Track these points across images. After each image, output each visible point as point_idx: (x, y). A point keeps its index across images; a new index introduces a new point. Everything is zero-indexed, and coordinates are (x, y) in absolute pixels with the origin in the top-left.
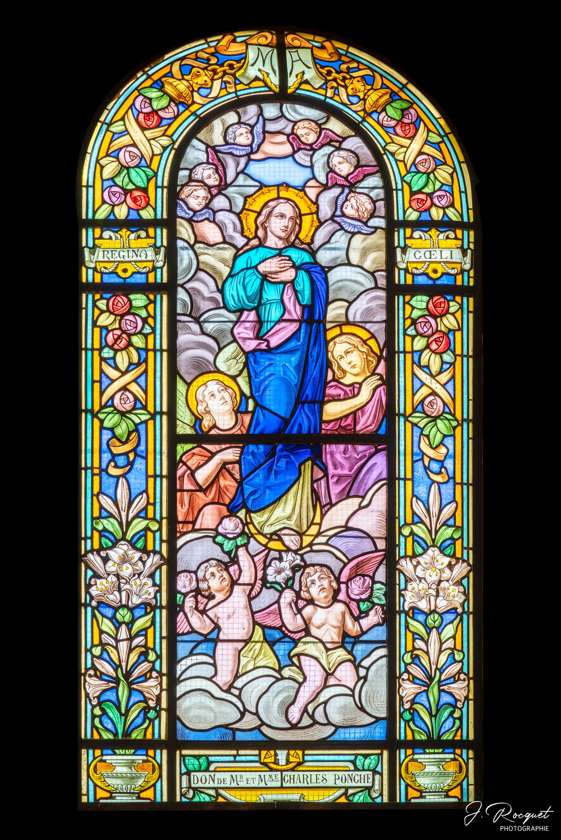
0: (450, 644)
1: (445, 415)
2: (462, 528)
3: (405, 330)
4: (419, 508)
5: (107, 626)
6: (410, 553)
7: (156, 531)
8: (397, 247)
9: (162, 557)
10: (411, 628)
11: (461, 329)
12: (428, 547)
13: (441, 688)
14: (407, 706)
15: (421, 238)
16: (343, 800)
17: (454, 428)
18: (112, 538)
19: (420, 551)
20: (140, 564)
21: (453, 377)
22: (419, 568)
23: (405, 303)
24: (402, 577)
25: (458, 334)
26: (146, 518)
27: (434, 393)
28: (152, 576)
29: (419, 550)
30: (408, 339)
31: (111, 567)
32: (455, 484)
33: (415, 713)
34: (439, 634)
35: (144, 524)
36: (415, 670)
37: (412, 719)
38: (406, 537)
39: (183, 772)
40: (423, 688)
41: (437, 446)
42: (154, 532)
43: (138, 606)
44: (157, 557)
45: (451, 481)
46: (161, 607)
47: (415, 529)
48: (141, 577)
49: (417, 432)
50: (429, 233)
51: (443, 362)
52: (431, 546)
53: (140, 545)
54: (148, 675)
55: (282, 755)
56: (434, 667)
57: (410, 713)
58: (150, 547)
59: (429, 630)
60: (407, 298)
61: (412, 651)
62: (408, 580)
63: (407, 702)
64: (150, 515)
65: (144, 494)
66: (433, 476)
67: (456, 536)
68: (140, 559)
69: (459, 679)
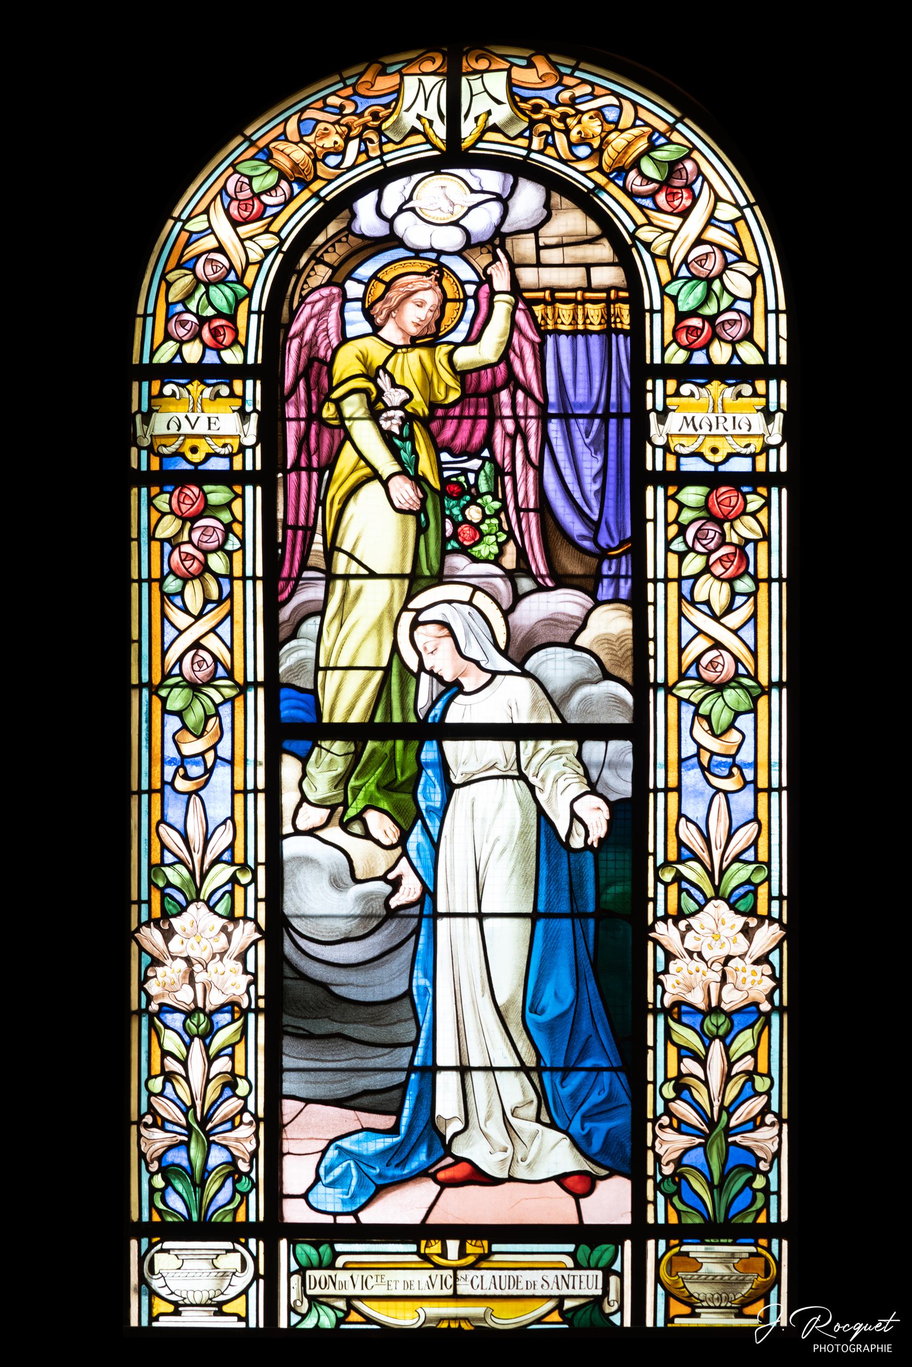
0: (747, 1063)
2: (768, 864)
3: (668, 543)
4: (689, 834)
6: (673, 909)
7: (249, 884)
8: (651, 411)
9: (258, 929)
10: (675, 1038)
11: (767, 537)
12: (708, 901)
15: (692, 395)
17: (755, 700)
19: (693, 907)
20: (223, 937)
22: (690, 935)
23: (667, 498)
25: (763, 547)
26: (232, 863)
27: (717, 645)
28: (242, 958)
29: (691, 906)
30: (673, 559)
32: (757, 791)
33: (683, 1182)
34: (727, 1048)
36: (682, 1109)
37: (678, 1193)
39: (292, 1270)
40: (698, 1141)
41: (724, 732)
44: (251, 925)
50: (708, 386)
52: (712, 898)
54: (237, 1120)
55: (453, 1246)
56: (716, 1104)
57: (674, 1182)
58: (239, 912)
59: (707, 1039)
60: (672, 490)
62: (670, 956)
63: (667, 1164)
64: (239, 859)
65: (229, 822)
66: (715, 781)
67: (757, 879)
68: (224, 929)
69: (763, 1124)
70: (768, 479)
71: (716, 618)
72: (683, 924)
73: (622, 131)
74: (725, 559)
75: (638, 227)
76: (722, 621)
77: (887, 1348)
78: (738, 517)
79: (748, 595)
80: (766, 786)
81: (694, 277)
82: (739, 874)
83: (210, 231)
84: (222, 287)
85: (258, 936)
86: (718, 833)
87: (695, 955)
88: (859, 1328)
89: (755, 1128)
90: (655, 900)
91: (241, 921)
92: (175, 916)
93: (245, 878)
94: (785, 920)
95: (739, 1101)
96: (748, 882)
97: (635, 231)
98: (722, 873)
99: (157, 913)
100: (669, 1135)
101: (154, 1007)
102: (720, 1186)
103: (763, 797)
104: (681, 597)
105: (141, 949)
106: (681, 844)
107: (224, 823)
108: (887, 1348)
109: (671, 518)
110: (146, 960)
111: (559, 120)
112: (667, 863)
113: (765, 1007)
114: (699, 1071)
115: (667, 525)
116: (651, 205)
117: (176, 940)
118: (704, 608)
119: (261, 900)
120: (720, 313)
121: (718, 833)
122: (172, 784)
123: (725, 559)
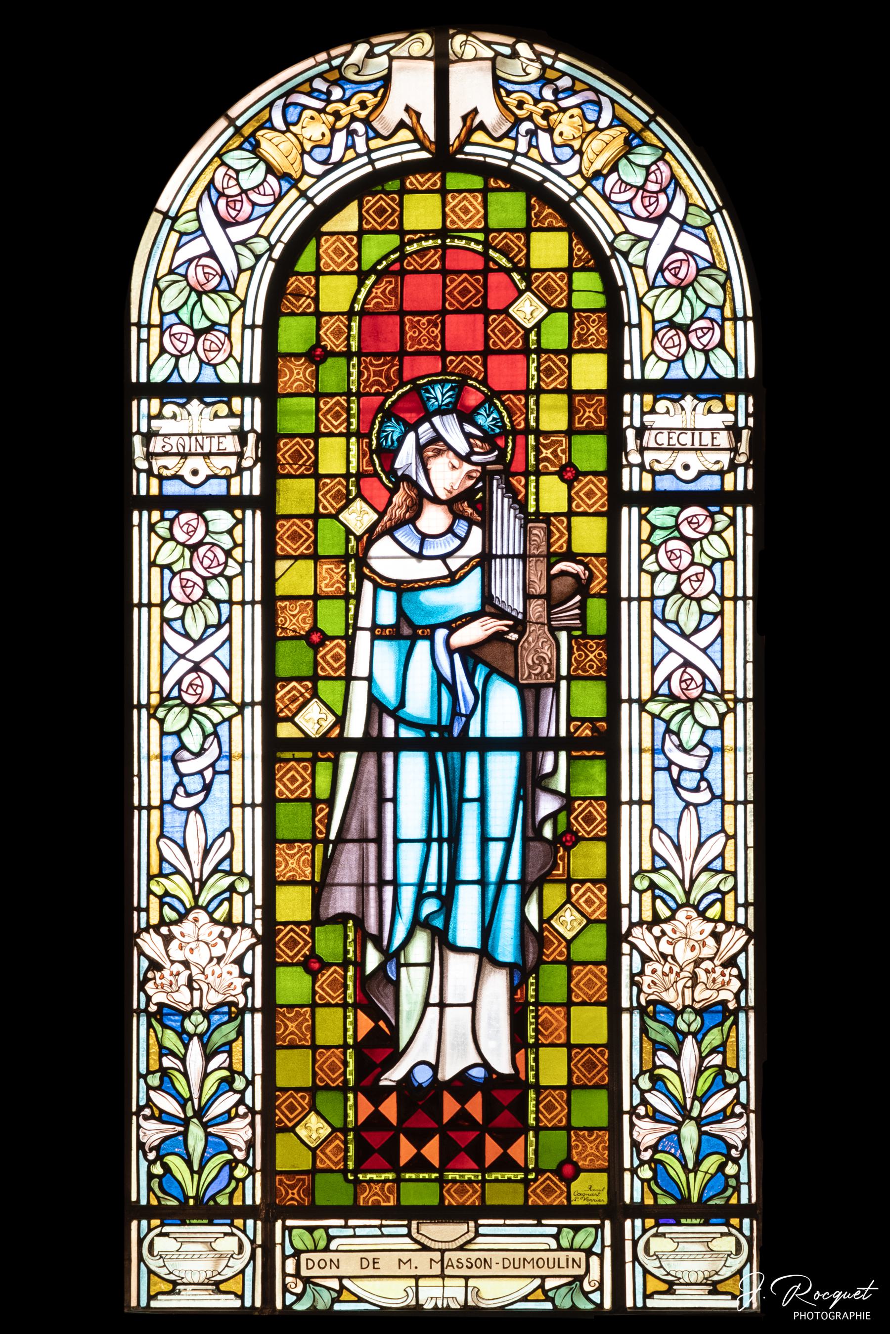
2: (734, 874)
3: (641, 562)
5: (171, 1040)
6: (648, 916)
7: (247, 893)
11: (733, 558)
13: (704, 1129)
14: (646, 1156)
17: (722, 717)
20: (221, 943)
21: (721, 634)
23: (642, 517)
25: (729, 565)
26: (230, 873)
27: (687, 664)
28: (239, 961)
29: (664, 912)
30: (646, 578)
31: (176, 953)
34: (699, 1043)
38: (641, 892)
44: (247, 932)
45: (717, 803)
46: (253, 1010)
48: (222, 964)
49: (660, 727)
50: (682, 402)
51: (702, 612)
53: (220, 915)
56: (689, 1095)
57: (651, 1168)
58: (237, 918)
60: (644, 510)
61: (651, 1071)
63: (646, 1150)
64: (237, 869)
65: (228, 834)
68: (221, 935)
70: (736, 498)
72: (656, 930)
74: (694, 578)
76: (692, 639)
77: (865, 1316)
79: (716, 615)
80: (732, 799)
81: (669, 286)
82: (707, 883)
83: (199, 233)
84: (212, 295)
85: (254, 940)
86: (688, 845)
87: (669, 959)
88: (838, 1296)
90: (629, 906)
91: (239, 928)
93: (243, 886)
94: (751, 926)
96: (717, 890)
97: (613, 241)
98: (692, 882)
99: (154, 920)
101: (153, 1008)
103: (729, 809)
104: (653, 616)
105: (141, 953)
106: (655, 853)
107: (222, 834)
108: (865, 1316)
109: (644, 537)
110: (145, 964)
112: (641, 871)
113: (732, 1005)
115: (641, 542)
117: (174, 945)
118: (674, 627)
119: (258, 907)
120: (693, 322)
121: (688, 845)
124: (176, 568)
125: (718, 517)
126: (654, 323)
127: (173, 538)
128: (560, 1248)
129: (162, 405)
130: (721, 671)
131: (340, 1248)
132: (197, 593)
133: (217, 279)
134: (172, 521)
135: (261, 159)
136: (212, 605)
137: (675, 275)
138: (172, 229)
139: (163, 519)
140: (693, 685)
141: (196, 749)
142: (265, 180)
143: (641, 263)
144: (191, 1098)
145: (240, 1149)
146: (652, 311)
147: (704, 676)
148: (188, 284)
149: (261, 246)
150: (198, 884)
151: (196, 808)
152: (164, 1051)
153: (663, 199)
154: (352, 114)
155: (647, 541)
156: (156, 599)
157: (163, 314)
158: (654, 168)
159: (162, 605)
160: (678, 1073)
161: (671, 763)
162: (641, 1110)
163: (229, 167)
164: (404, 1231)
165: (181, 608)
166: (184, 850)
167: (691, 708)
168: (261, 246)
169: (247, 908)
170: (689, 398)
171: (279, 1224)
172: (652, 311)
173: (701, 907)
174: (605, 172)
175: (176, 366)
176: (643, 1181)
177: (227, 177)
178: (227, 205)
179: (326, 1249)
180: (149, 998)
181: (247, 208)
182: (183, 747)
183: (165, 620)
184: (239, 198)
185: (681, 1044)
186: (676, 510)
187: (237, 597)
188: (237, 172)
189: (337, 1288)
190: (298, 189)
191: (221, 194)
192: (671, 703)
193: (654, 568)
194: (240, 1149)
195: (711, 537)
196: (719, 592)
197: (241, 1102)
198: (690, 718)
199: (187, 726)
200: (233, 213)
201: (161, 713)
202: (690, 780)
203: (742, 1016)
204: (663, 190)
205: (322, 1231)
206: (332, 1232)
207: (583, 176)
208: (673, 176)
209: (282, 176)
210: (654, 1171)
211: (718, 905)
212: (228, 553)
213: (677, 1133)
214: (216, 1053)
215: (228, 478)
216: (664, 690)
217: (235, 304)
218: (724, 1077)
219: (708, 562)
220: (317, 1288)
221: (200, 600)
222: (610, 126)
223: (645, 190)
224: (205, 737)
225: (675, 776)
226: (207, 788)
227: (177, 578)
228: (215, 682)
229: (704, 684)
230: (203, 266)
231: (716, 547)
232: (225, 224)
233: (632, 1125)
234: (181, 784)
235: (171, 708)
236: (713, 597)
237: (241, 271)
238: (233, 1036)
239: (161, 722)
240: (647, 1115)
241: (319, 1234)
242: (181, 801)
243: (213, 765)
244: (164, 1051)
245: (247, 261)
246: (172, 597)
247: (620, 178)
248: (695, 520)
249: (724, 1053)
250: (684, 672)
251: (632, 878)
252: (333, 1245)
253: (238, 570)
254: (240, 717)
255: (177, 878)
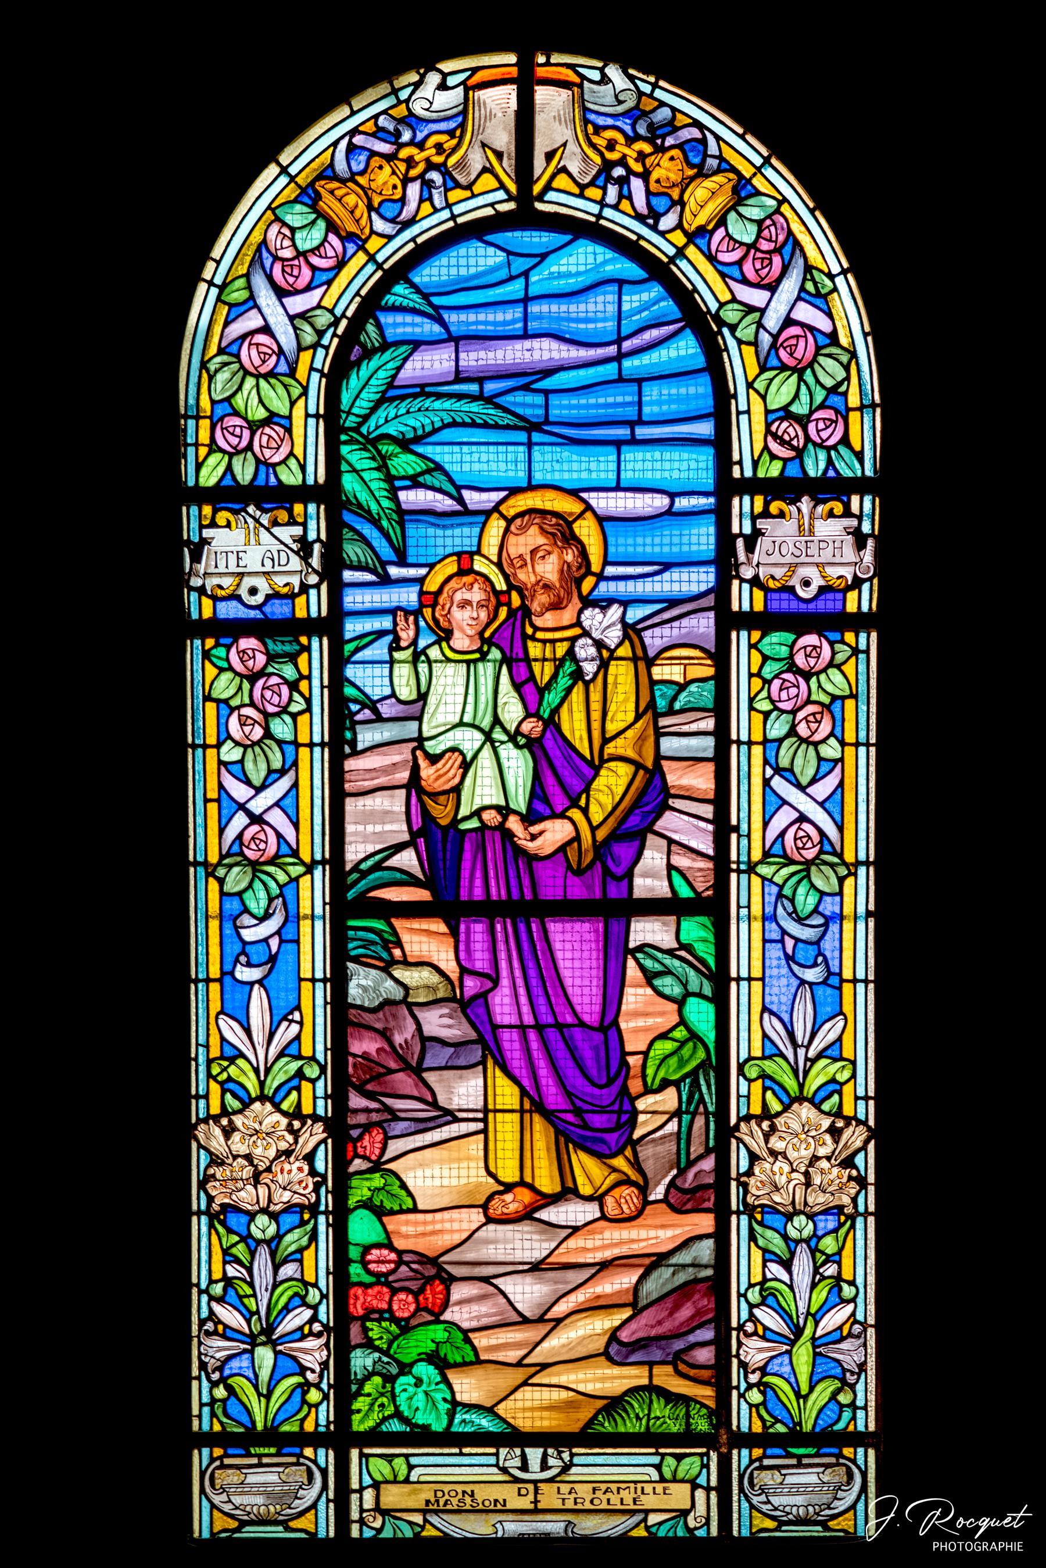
1: (823, 857)
3: (751, 700)
6: (756, 1109)
11: (854, 696)
14: (754, 1378)
16: (641, 1532)
17: (841, 880)
18: (242, 1093)
24: (743, 1152)
25: (850, 704)
26: (299, 1057)
27: (802, 818)
29: (775, 1106)
30: (758, 718)
35: (295, 1065)
36: (768, 1317)
40: (785, 1348)
42: (313, 1081)
43: (289, 1208)
47: (769, 1066)
51: (820, 759)
57: (760, 1391)
58: (307, 1109)
63: (753, 1372)
64: (307, 1052)
67: (842, 1077)
71: (802, 788)
72: (765, 1125)
73: (707, 176)
74: (811, 718)
75: (722, 305)
76: (808, 790)
78: (824, 670)
79: (836, 761)
89: (842, 1339)
92: (235, 1113)
93: (312, 1071)
94: (871, 1123)
95: (825, 1308)
96: (833, 1081)
99: (215, 1110)
100: (755, 1343)
102: (806, 1397)
104: (766, 762)
109: (755, 670)
111: (636, 160)
112: (750, 1058)
114: (785, 1277)
115: (751, 675)
116: (737, 274)
117: (236, 1137)
122: (232, 973)
123: (811, 718)
124: (235, 703)
125: (838, 647)
126: (767, 412)
127: (231, 668)
128: (662, 1479)
129: (215, 512)
130: (841, 828)
131: (422, 1479)
132: (258, 733)
133: (274, 358)
134: (228, 648)
135: (320, 214)
136: (276, 748)
137: (791, 354)
138: (219, 299)
139: (217, 645)
140: (809, 845)
141: (260, 912)
142: (325, 240)
143: (752, 339)
144: (258, 1312)
145: (313, 1371)
146: (764, 398)
147: (822, 833)
148: (242, 367)
149: (323, 319)
150: (263, 1072)
151: (260, 982)
152: (228, 1258)
153: (777, 260)
154: (427, 160)
155: (759, 675)
156: (212, 740)
157: (213, 402)
158: (768, 222)
159: (218, 746)
160: (791, 1287)
161: (784, 932)
162: (749, 1327)
163: (284, 224)
164: (492, 1460)
165: (241, 750)
166: (248, 1031)
167: (808, 870)
168: (323, 319)
169: (314, 1097)
170: (805, 499)
171: (354, 1453)
172: (764, 398)
173: (817, 1101)
174: (710, 227)
175: (229, 468)
176: (751, 1406)
177: (280, 237)
178: (283, 271)
179: (407, 1481)
180: (210, 1199)
181: (306, 273)
182: (246, 910)
183: (221, 763)
184: (296, 262)
185: (792, 1254)
186: (790, 637)
187: (304, 738)
188: (293, 230)
189: (421, 1522)
190: (366, 252)
191: (276, 258)
192: (785, 865)
193: (766, 706)
194: (313, 1371)
195: (830, 671)
196: (839, 736)
197: (314, 1319)
198: (805, 881)
199: (250, 886)
200: (291, 280)
201: (221, 872)
202: (805, 954)
203: (860, 1222)
204: (778, 250)
205: (402, 1460)
206: (413, 1461)
207: (685, 233)
208: (790, 233)
209: (348, 238)
210: (763, 1393)
211: (836, 1098)
212: (293, 686)
213: (789, 1353)
214: (285, 1261)
215: (292, 596)
216: (777, 849)
217: (296, 391)
218: (840, 1289)
219: (826, 700)
220: (397, 1522)
221: (260, 741)
222: (718, 171)
223: (758, 250)
224: (271, 900)
225: (790, 951)
226: (273, 959)
227: (235, 714)
228: (279, 836)
229: (821, 842)
230: (257, 345)
231: (835, 682)
232: (281, 293)
233: (740, 1344)
234: (243, 952)
235: (230, 867)
236: (832, 741)
237: (300, 349)
238: (304, 1241)
239: (221, 881)
240: (755, 1333)
241: (399, 1462)
242: (244, 974)
243: (278, 932)
244: (228, 1258)
245: (309, 338)
246: (229, 737)
247: (728, 234)
248: (814, 654)
249: (839, 1263)
250: (799, 828)
251: (741, 1067)
252: (414, 1476)
253: (304, 706)
254: (309, 877)
255: (240, 1062)
